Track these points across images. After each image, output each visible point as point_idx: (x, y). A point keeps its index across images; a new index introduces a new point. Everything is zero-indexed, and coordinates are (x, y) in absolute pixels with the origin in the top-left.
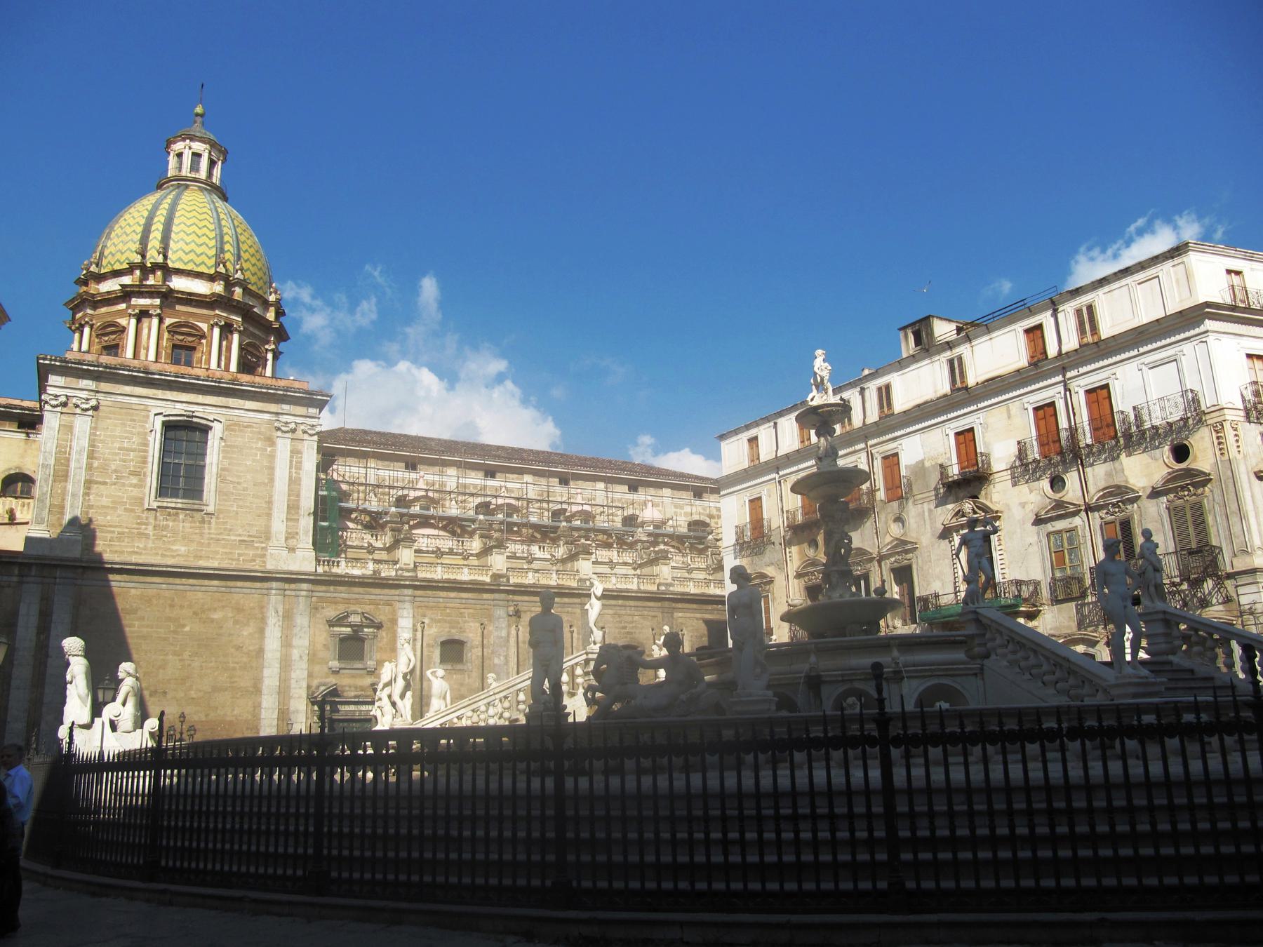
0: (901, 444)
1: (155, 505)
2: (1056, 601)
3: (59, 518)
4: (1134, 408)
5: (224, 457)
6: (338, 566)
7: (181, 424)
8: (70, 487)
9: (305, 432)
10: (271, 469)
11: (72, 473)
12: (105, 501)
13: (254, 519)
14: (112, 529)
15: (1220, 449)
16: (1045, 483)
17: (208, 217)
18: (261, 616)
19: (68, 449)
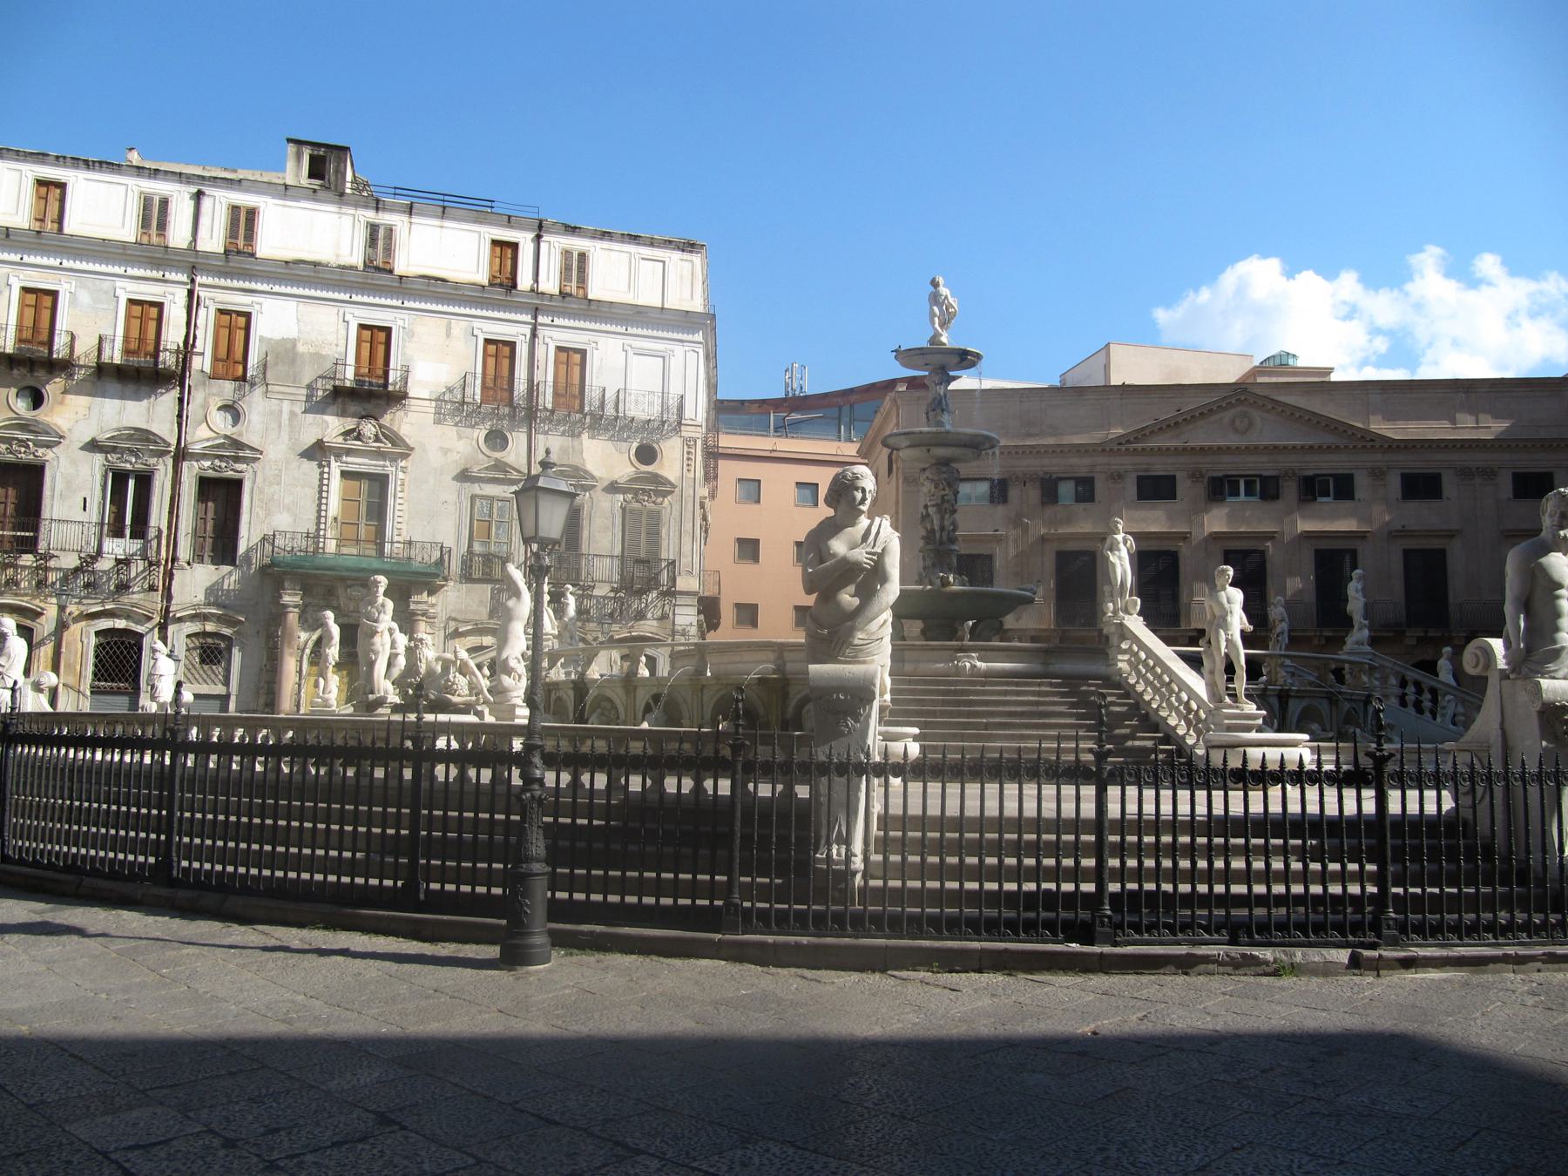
2: (467, 577)
15: (688, 465)
16: (481, 433)
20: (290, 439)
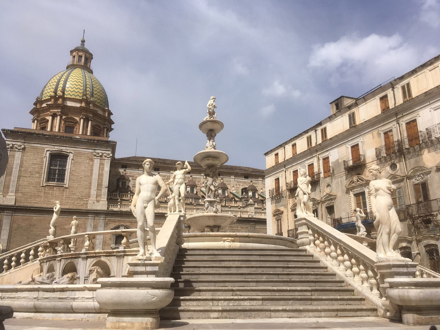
0: (330, 153)
1: (45, 185)
3: (7, 190)
4: (427, 129)
5: (73, 166)
6: (117, 207)
7: (57, 154)
8: (12, 178)
9: (105, 156)
10: (92, 170)
11: (13, 173)
12: (25, 183)
13: (84, 189)
14: (28, 194)
17: (81, 78)
18: (84, 227)
19: (12, 164)
20: (341, 189)
